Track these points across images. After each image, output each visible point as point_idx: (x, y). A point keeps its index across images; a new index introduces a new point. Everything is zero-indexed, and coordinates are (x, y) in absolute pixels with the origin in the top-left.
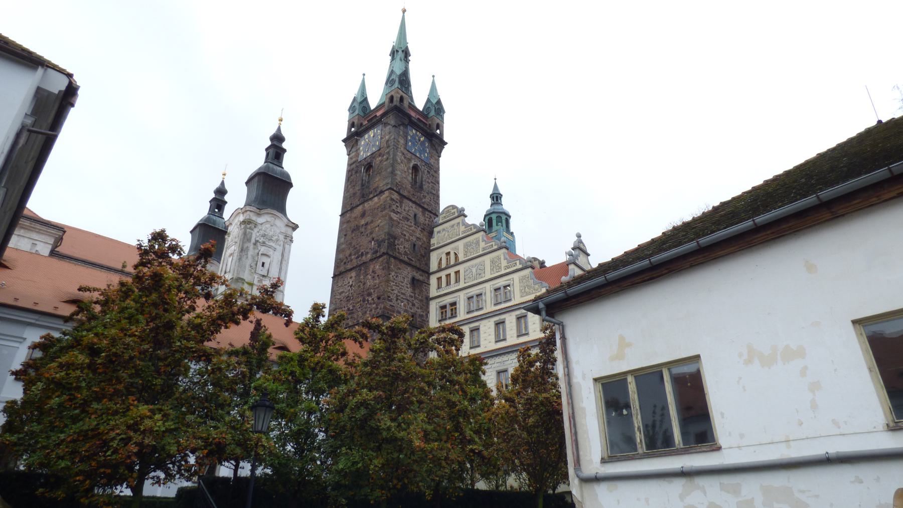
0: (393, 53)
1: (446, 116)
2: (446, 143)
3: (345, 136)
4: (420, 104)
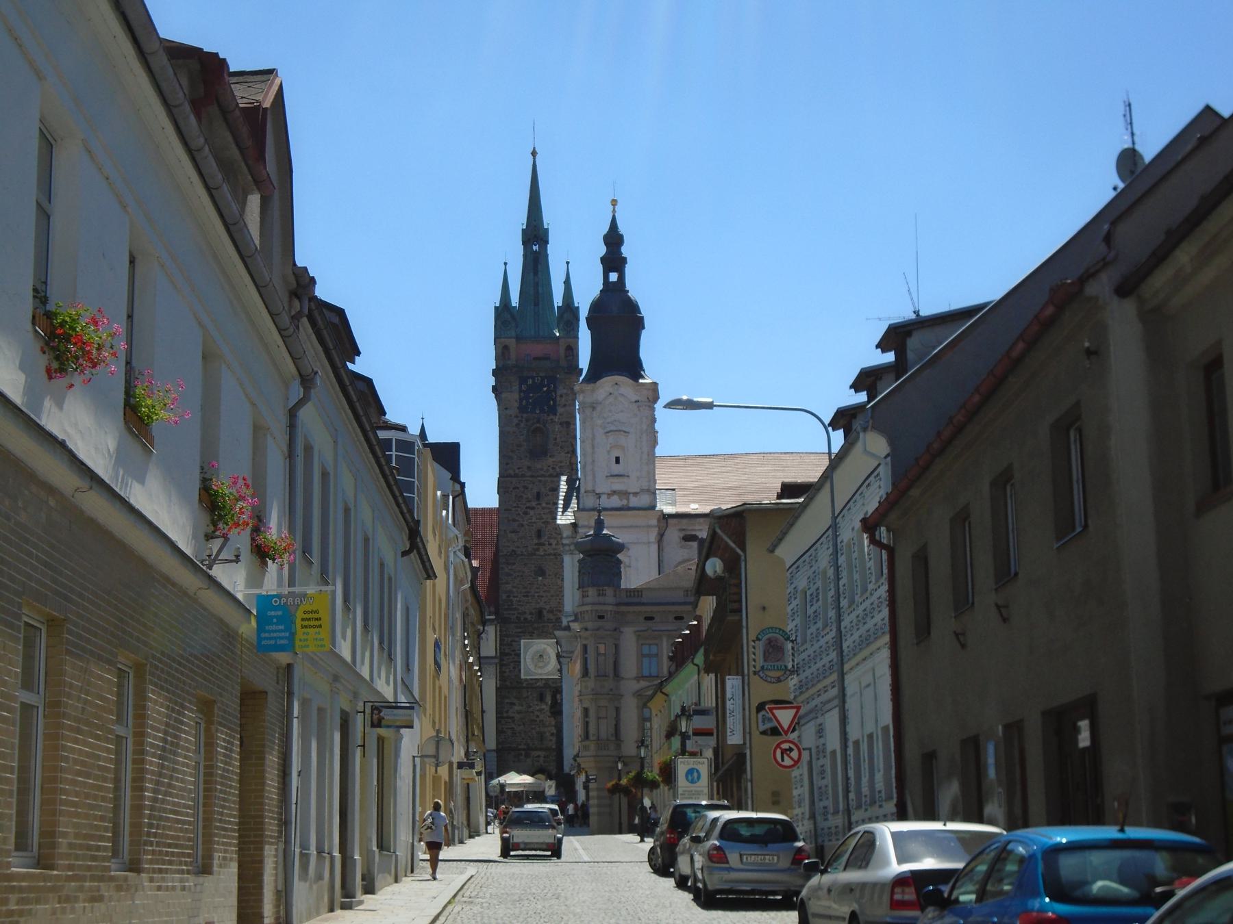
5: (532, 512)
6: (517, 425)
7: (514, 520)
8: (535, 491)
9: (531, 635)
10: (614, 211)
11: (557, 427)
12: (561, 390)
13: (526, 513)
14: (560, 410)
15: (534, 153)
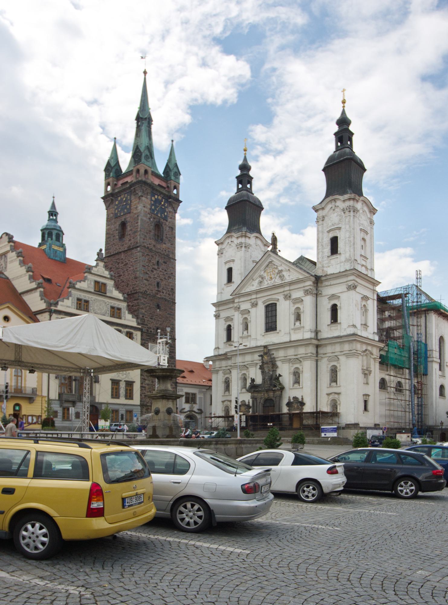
6: (149, 219)
7: (147, 273)
8: (157, 260)
10: (344, 107)
11: (168, 228)
13: (152, 271)
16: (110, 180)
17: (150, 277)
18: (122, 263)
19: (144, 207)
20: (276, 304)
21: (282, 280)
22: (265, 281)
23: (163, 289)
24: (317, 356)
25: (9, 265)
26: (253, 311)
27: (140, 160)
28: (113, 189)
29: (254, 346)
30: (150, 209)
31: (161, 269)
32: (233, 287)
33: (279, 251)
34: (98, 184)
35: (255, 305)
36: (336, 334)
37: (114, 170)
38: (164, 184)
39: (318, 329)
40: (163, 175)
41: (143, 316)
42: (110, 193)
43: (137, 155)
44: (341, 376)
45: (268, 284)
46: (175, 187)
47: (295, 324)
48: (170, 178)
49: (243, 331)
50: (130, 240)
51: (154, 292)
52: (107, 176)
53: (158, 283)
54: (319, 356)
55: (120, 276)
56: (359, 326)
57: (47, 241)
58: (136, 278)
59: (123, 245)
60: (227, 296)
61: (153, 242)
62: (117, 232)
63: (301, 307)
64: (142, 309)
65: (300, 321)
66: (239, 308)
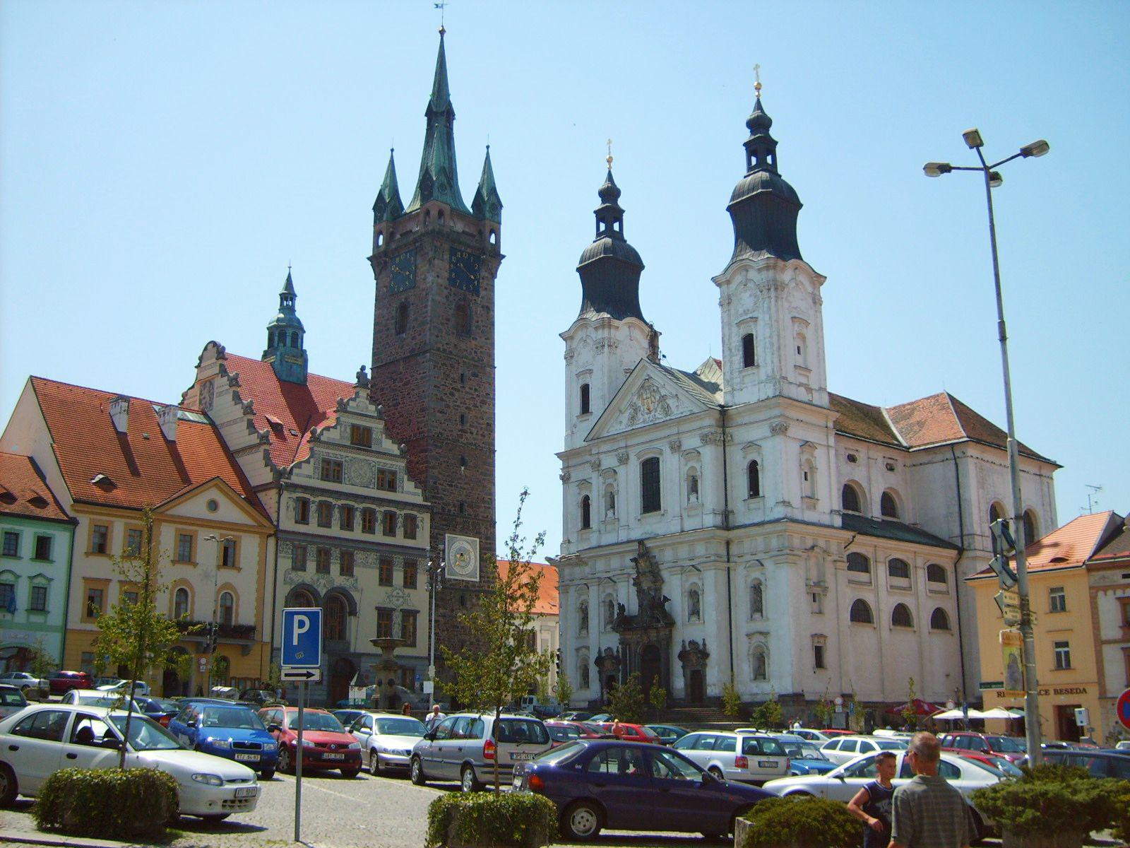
0: (430, 113)
1: (505, 213)
2: (504, 257)
3: (370, 254)
4: (468, 199)
5: (457, 394)
8: (460, 372)
9: (454, 531)
11: (479, 309)
12: (484, 274)
14: (483, 293)
15: (442, 32)
16: (384, 225)
17: (448, 406)
18: (401, 380)
19: (438, 276)
20: (658, 459)
21: (667, 414)
22: (639, 415)
23: (471, 426)
24: (728, 561)
25: (216, 401)
26: (621, 470)
27: (431, 194)
28: (387, 242)
29: (625, 540)
30: (448, 279)
31: (467, 389)
32: (593, 419)
33: (664, 356)
34: (361, 237)
35: (624, 460)
36: (757, 520)
37: (389, 209)
38: (472, 230)
39: (730, 508)
40: (471, 211)
41: (435, 483)
42: (382, 249)
43: (425, 185)
44: (769, 596)
45: (644, 422)
46: (492, 231)
47: (689, 499)
48: (484, 215)
49: (606, 510)
50: (414, 338)
51: (454, 433)
52: (377, 220)
53: (462, 417)
54: (731, 559)
55: (398, 404)
56: (796, 502)
57: (276, 349)
58: (423, 410)
59: (402, 347)
60: (579, 443)
61: (454, 341)
62: (393, 321)
63: (697, 466)
64: (433, 468)
65: (697, 493)
66: (599, 465)
